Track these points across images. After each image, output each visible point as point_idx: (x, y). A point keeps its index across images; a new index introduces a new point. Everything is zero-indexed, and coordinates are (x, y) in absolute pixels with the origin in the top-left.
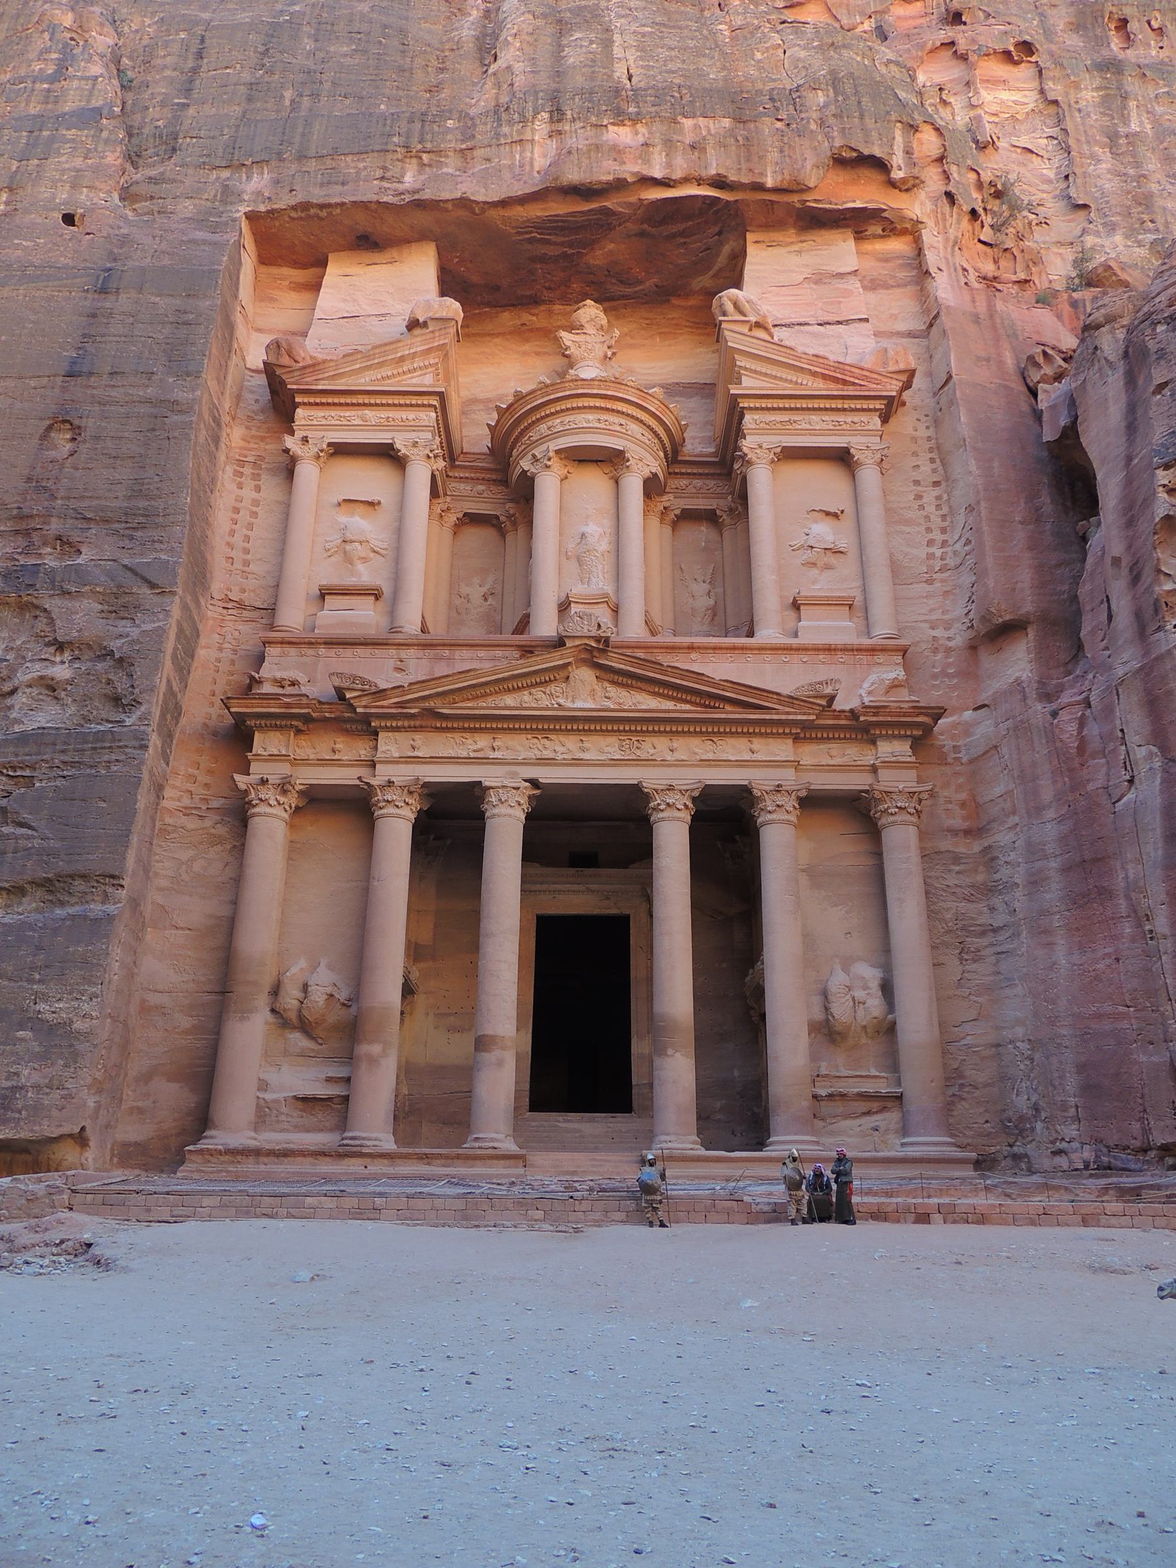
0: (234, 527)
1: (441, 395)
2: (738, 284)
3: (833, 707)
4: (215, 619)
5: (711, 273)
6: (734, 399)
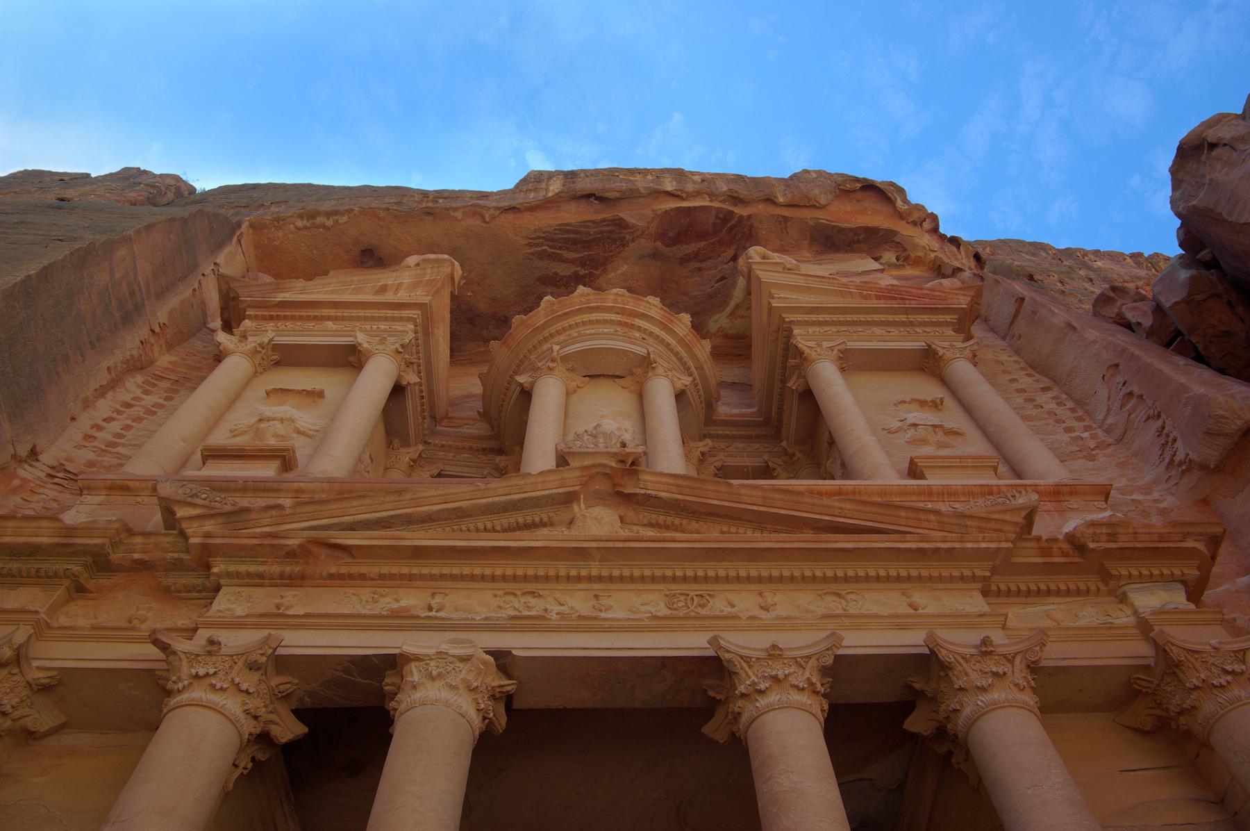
0: (115, 415)
1: (421, 306)
3: (1035, 532)
4: (24, 480)
5: (728, 310)
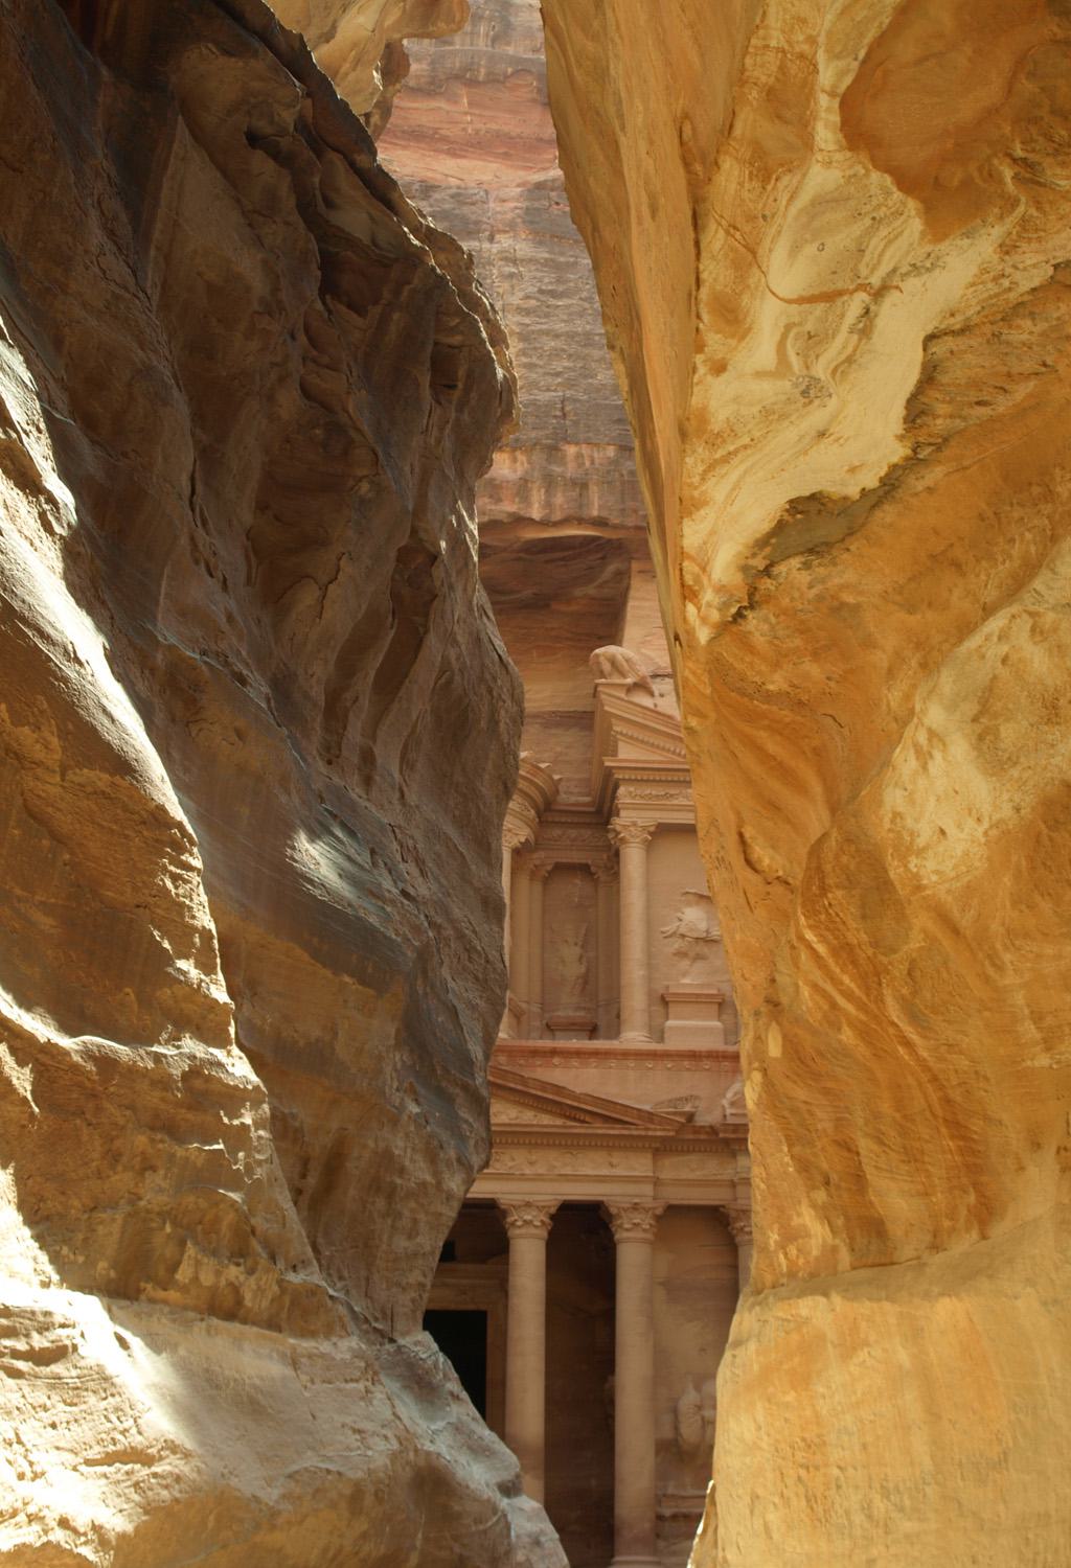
2: (613, 636)
5: (596, 583)
6: (609, 772)
